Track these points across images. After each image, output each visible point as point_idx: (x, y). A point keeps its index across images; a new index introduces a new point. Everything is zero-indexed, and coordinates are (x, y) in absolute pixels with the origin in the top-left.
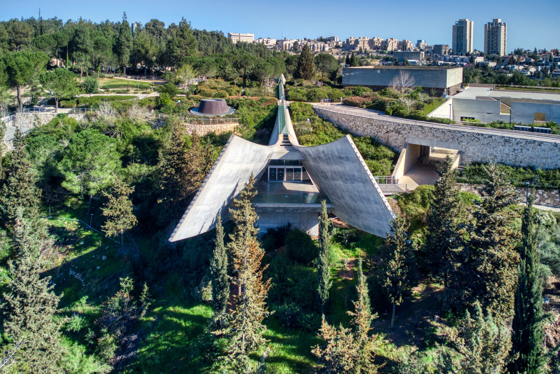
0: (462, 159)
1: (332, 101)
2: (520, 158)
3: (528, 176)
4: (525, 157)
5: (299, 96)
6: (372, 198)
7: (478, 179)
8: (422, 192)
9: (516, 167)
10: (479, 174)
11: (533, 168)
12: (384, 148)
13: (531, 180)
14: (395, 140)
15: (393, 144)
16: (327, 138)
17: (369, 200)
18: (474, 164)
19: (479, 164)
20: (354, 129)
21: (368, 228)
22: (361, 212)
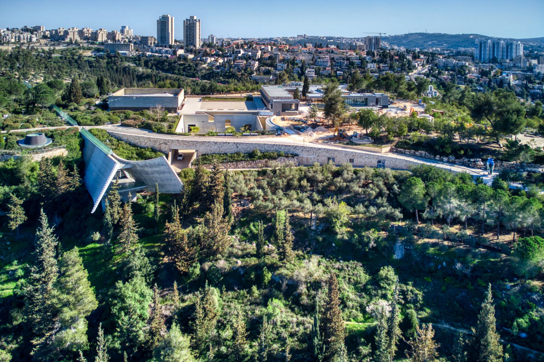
0: (197, 154)
1: (112, 123)
2: (221, 150)
3: (224, 157)
4: (223, 150)
5: (89, 122)
6: (173, 179)
7: (205, 162)
8: (184, 172)
9: (220, 154)
10: (205, 160)
11: (226, 154)
12: (159, 153)
13: (226, 159)
14: (164, 148)
15: (163, 150)
16: (125, 151)
17: (171, 180)
18: (203, 155)
19: (205, 155)
20: (139, 144)
21: (169, 191)
22: (166, 185)
